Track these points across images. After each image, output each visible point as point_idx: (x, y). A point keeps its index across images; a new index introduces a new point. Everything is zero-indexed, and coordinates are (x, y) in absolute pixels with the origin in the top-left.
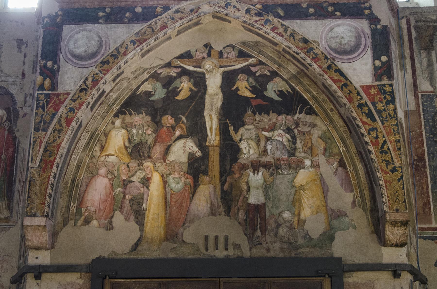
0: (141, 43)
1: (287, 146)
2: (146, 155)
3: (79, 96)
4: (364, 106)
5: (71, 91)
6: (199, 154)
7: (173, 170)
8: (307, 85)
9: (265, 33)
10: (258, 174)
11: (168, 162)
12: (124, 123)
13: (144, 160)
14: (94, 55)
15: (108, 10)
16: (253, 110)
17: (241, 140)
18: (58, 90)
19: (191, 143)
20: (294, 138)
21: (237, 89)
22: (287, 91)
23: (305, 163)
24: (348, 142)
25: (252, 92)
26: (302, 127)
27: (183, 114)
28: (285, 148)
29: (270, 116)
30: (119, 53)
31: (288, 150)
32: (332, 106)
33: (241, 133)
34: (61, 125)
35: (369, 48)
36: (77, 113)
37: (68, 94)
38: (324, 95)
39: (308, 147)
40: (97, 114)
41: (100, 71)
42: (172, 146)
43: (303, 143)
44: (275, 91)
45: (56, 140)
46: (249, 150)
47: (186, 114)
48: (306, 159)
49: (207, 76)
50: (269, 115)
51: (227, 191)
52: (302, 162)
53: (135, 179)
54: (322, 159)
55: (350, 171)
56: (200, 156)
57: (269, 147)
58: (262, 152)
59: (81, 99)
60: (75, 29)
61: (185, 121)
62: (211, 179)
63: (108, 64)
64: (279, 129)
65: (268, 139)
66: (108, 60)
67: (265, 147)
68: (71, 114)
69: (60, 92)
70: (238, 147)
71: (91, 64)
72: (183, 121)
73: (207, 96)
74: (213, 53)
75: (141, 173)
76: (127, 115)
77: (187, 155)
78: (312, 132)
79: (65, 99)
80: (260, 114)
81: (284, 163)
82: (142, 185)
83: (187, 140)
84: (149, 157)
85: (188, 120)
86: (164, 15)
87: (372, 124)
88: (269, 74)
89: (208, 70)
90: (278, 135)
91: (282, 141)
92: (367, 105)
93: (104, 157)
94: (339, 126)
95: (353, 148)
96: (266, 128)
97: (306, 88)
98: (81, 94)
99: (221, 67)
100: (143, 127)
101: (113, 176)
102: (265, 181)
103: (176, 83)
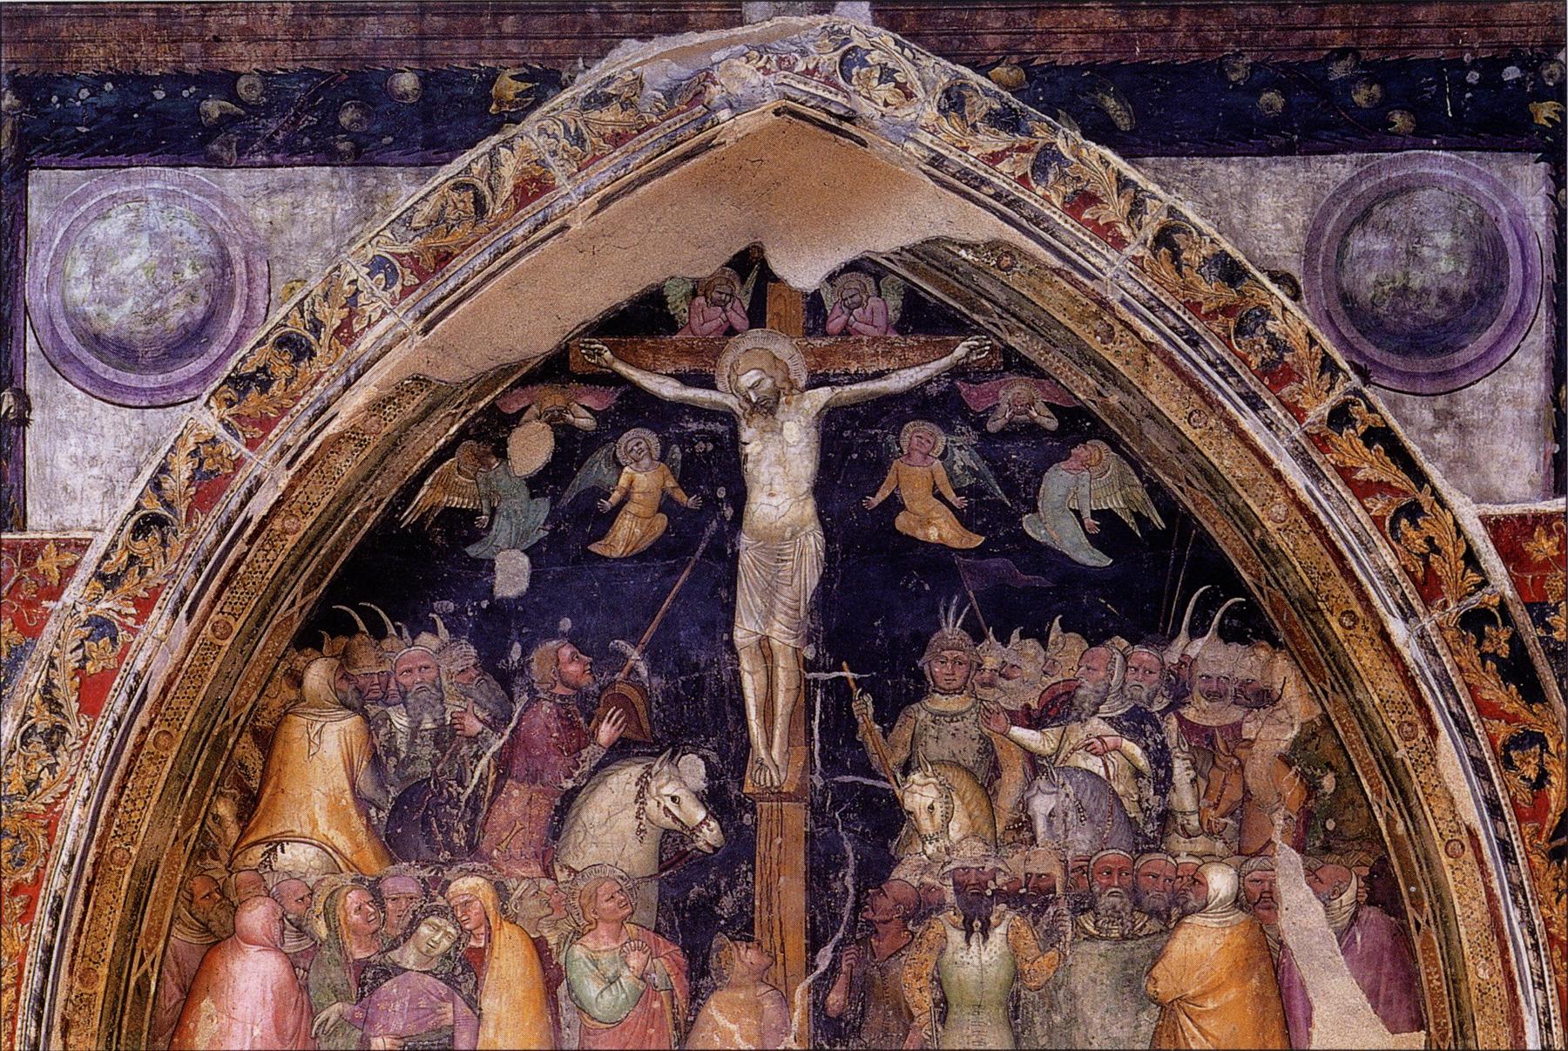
0: (423, 275)
1: (1125, 801)
2: (458, 840)
3: (133, 559)
4: (1493, 621)
5: (95, 530)
6: (711, 834)
7: (590, 916)
8: (1234, 483)
9: (1037, 225)
10: (986, 937)
11: (562, 876)
12: (346, 677)
13: (450, 863)
14: (192, 338)
15: (251, 87)
16: (971, 616)
17: (907, 769)
18: (31, 522)
19: (670, 780)
20: (1161, 758)
21: (895, 504)
22: (1138, 516)
23: (1205, 885)
24: (1415, 780)
25: (965, 519)
26: (1204, 704)
27: (633, 636)
28: (1116, 811)
29: (1051, 647)
30: (317, 327)
31: (1131, 822)
32: (1353, 599)
33: (908, 735)
34: (54, 705)
35: (1543, 311)
36: (127, 646)
37: (82, 546)
38: (1315, 539)
39: (1223, 807)
40: (214, 630)
41: (227, 426)
42: (581, 797)
43: (1202, 783)
44: (1078, 513)
45: (37, 781)
46: (948, 818)
47: (647, 636)
48: (1215, 867)
49: (747, 434)
50: (1043, 640)
51: (839, 1018)
52: (1198, 881)
53: (408, 956)
54: (1288, 870)
55: (1418, 925)
56: (716, 849)
57: (1042, 805)
58: (1007, 829)
59: (143, 571)
60: (88, 193)
61: (643, 670)
62: (767, 961)
63: (265, 386)
64: (1094, 713)
65: (1035, 764)
66: (263, 370)
67: (1024, 804)
68: (101, 656)
69: (38, 536)
70: (895, 802)
71: (181, 386)
72: (633, 670)
73: (745, 540)
74: (773, 307)
75: (438, 929)
76: (358, 638)
77: (651, 844)
78: (1249, 730)
79: (68, 572)
80: (1004, 639)
81: (1109, 886)
82: (442, 988)
83: (651, 767)
84: (473, 848)
85: (653, 671)
86: (530, 124)
87: (1524, 714)
88: (1052, 424)
89: (754, 400)
90: (1089, 748)
91: (1102, 773)
92: (1508, 619)
93: (259, 850)
94: (1377, 701)
95: (1437, 813)
96: (1027, 707)
97: (1232, 497)
98: (140, 546)
99: (816, 382)
100: (442, 700)
101: (306, 944)
102: (1017, 975)
103: (595, 470)
